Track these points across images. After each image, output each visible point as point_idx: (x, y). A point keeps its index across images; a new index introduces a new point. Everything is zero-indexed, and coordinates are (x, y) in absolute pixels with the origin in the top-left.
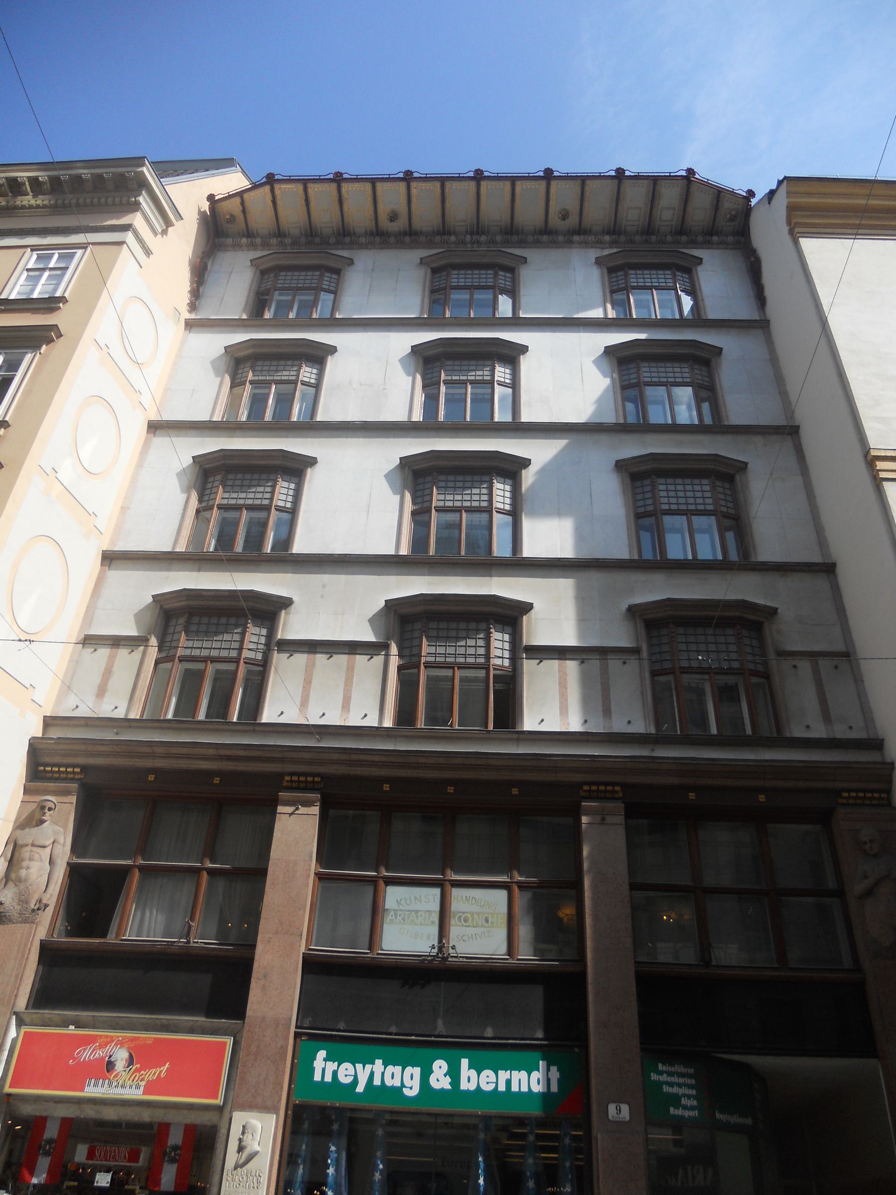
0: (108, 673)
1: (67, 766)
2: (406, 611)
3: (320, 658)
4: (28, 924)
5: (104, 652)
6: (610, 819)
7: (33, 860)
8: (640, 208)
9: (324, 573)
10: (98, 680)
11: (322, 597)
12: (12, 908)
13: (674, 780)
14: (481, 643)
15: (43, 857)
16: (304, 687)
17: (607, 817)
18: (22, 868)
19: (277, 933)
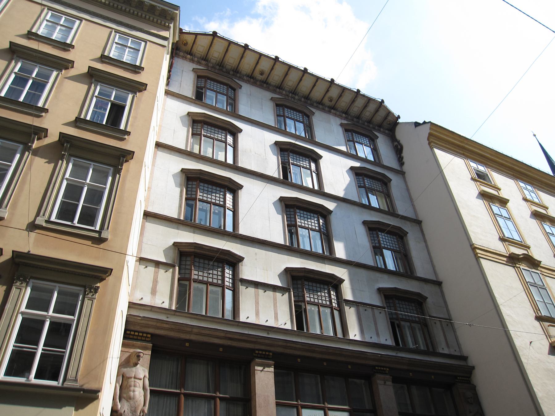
0: (155, 282)
1: (143, 333)
2: (295, 274)
3: (261, 291)
5: (151, 269)
6: (388, 383)
8: (359, 108)
9: (255, 247)
10: (151, 285)
11: (256, 259)
13: (405, 367)
14: (220, 273)
16: (256, 305)
17: (386, 382)
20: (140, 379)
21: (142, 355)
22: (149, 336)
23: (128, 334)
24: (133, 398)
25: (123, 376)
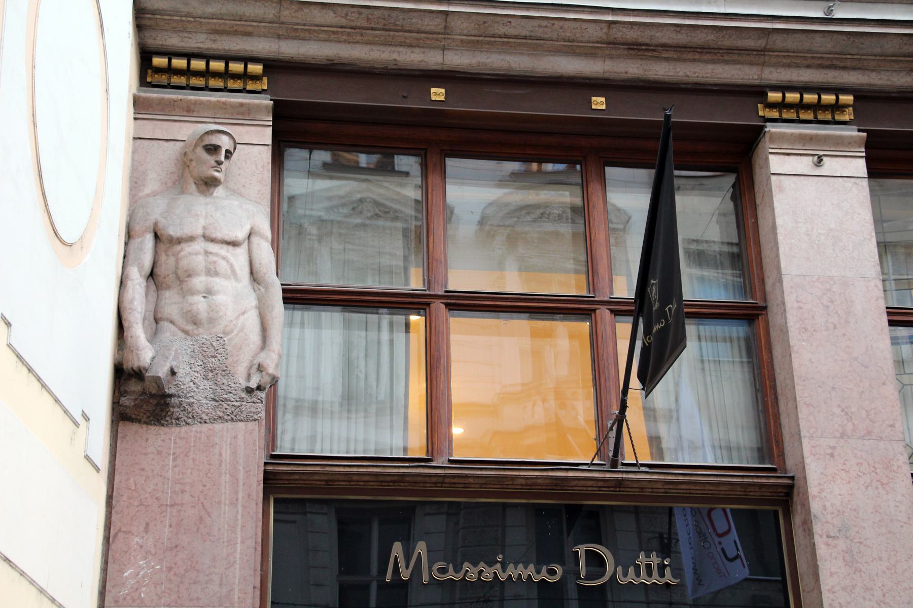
1: (227, 59)
4: (241, 425)
7: (216, 274)
12: (191, 384)
15: (237, 267)
18: (193, 293)
19: (843, 435)
20: (234, 244)
21: (225, 142)
22: (256, 68)
23: (159, 70)
24: (212, 321)
25: (156, 236)
